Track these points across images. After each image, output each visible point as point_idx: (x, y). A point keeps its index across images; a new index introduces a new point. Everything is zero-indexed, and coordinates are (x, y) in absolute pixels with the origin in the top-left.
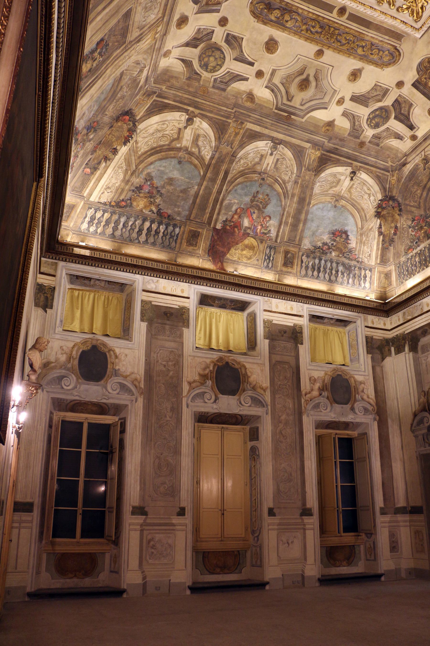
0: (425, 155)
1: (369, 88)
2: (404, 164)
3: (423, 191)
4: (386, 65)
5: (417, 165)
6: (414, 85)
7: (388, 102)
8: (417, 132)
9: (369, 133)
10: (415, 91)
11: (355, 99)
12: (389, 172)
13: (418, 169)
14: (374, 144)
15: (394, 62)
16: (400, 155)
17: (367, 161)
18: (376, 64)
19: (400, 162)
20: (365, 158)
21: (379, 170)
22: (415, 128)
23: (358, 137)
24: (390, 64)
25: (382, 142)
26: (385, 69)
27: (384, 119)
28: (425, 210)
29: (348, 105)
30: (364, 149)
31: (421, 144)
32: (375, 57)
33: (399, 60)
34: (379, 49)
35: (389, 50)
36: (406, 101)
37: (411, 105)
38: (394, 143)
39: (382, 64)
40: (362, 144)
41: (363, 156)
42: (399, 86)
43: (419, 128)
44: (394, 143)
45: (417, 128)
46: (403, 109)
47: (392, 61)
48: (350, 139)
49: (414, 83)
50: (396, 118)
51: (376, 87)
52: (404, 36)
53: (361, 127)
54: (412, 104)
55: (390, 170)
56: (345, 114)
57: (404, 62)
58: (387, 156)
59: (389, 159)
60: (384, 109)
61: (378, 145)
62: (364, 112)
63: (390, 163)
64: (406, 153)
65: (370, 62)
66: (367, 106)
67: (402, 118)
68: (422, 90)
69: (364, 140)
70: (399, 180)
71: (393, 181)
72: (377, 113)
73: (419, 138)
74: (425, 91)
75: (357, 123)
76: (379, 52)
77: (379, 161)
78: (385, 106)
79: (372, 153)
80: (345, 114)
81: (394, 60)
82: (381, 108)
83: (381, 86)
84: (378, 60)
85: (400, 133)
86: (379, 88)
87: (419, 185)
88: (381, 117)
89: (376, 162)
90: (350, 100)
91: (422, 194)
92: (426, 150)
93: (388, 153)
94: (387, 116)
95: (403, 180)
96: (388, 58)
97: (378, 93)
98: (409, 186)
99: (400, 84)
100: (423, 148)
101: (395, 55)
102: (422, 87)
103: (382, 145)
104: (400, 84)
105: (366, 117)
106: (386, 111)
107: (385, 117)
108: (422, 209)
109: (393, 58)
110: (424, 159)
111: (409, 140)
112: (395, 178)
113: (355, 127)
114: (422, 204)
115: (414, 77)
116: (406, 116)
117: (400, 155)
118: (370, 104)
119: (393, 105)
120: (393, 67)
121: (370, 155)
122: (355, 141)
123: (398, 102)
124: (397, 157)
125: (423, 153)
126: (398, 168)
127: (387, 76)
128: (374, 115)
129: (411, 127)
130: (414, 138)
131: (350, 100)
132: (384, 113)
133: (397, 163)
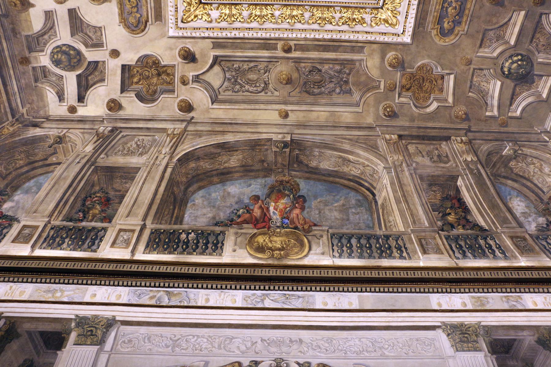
0: (64, 134)
1: (93, 23)
2: (36, 125)
3: (26, 165)
4: (125, 25)
5: (47, 137)
6: (124, 67)
7: (90, 55)
8: (81, 108)
9: (44, 60)
10: (119, 72)
11: (73, 14)
12: (13, 118)
13: (44, 141)
14: (34, 75)
15: (133, 31)
16: (42, 113)
17: (8, 83)
18: (121, 13)
19: (34, 120)
20: (10, 77)
21: (7, 105)
22: (83, 103)
23: (30, 50)
24: (129, 28)
25: (42, 83)
26: (122, 26)
27: (70, 65)
28: (7, 186)
29: (62, 11)
30: (21, 67)
31: (72, 121)
32: (128, 7)
33: (138, 34)
34: (137, 4)
35: (141, 16)
36: (102, 72)
37: (103, 80)
38: (51, 96)
39: (124, 19)
40: (25, 61)
41: (12, 72)
42: (112, 54)
43: (86, 106)
44: (51, 96)
45: (85, 104)
46: (92, 76)
47: (133, 28)
48: (22, 41)
49: (125, 65)
50: (78, 76)
51: (98, 29)
52: (162, 22)
53: (45, 44)
54: (104, 80)
55: (17, 117)
56: (49, 15)
57: (139, 39)
58: (30, 101)
59: (28, 106)
60: (80, 57)
61: (36, 81)
62: (64, 36)
63: (24, 111)
64: (50, 116)
65: (121, 4)
66: (72, 35)
67: (84, 83)
68: (124, 77)
69: (32, 60)
70: (13, 135)
71: (6, 130)
72: (72, 52)
73: (76, 114)
74: (127, 81)
75: (46, 37)
76: (134, 7)
77: (18, 96)
78: (83, 55)
79: (23, 81)
80: (49, 15)
81: (135, 29)
82: (79, 53)
83: (102, 35)
84: (126, 11)
85: (66, 94)
86: (99, 34)
87: (27, 157)
88: (70, 60)
89: (14, 94)
90: (69, 10)
91: (21, 167)
92: (71, 131)
93: (35, 98)
94: (74, 66)
95: (17, 139)
96: (134, 21)
97: (93, 37)
98: (17, 149)
99: (115, 53)
100: (70, 126)
101: (140, 26)
102: (127, 75)
103: (40, 85)
104: (115, 53)
105: (59, 43)
106: (79, 61)
107: (72, 64)
108: (6, 182)
109: (137, 26)
110: (59, 137)
111: (67, 107)
112: (11, 129)
113: (41, 39)
114: (10, 178)
115: (131, 60)
116: (88, 85)
117: (42, 113)
118: (77, 37)
119: (90, 62)
120: (127, 33)
121: (18, 80)
122: (23, 50)
123: (97, 66)
124: (38, 112)
125: (65, 131)
126: (26, 123)
127: (115, 34)
128: (67, 50)
129: (81, 99)
130: (72, 110)
131: (69, 10)
132: (75, 60)
133: (31, 118)
